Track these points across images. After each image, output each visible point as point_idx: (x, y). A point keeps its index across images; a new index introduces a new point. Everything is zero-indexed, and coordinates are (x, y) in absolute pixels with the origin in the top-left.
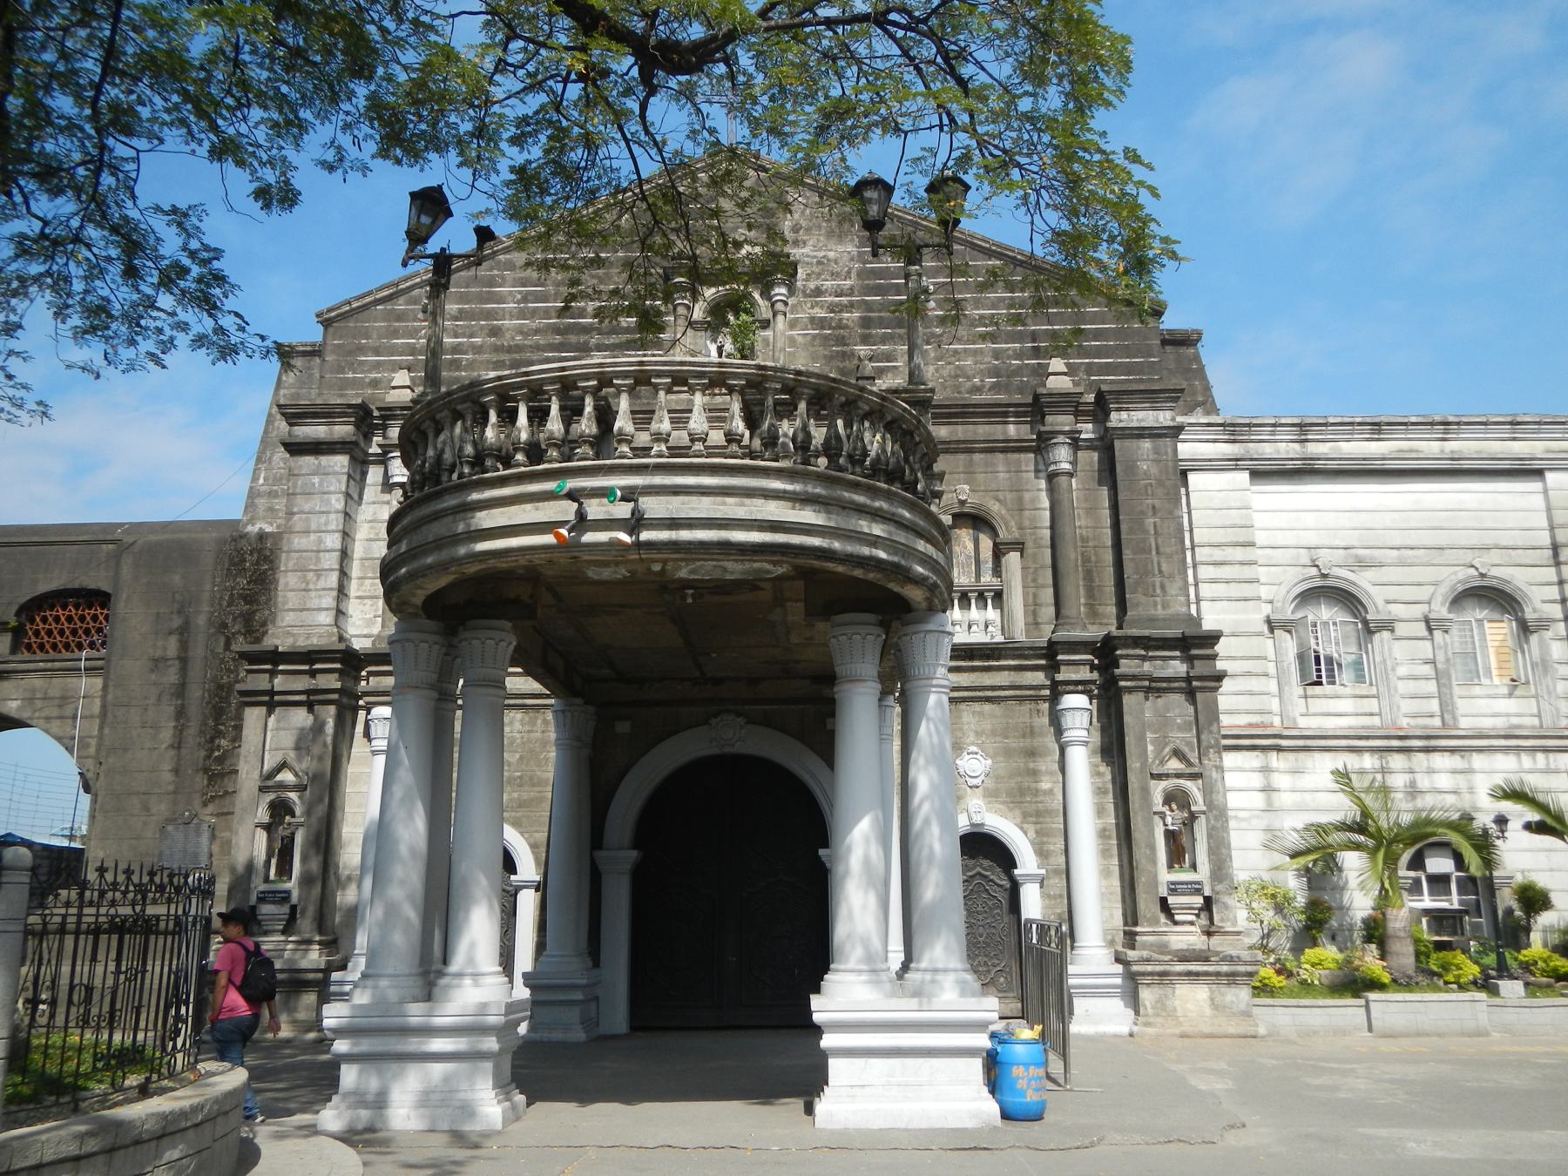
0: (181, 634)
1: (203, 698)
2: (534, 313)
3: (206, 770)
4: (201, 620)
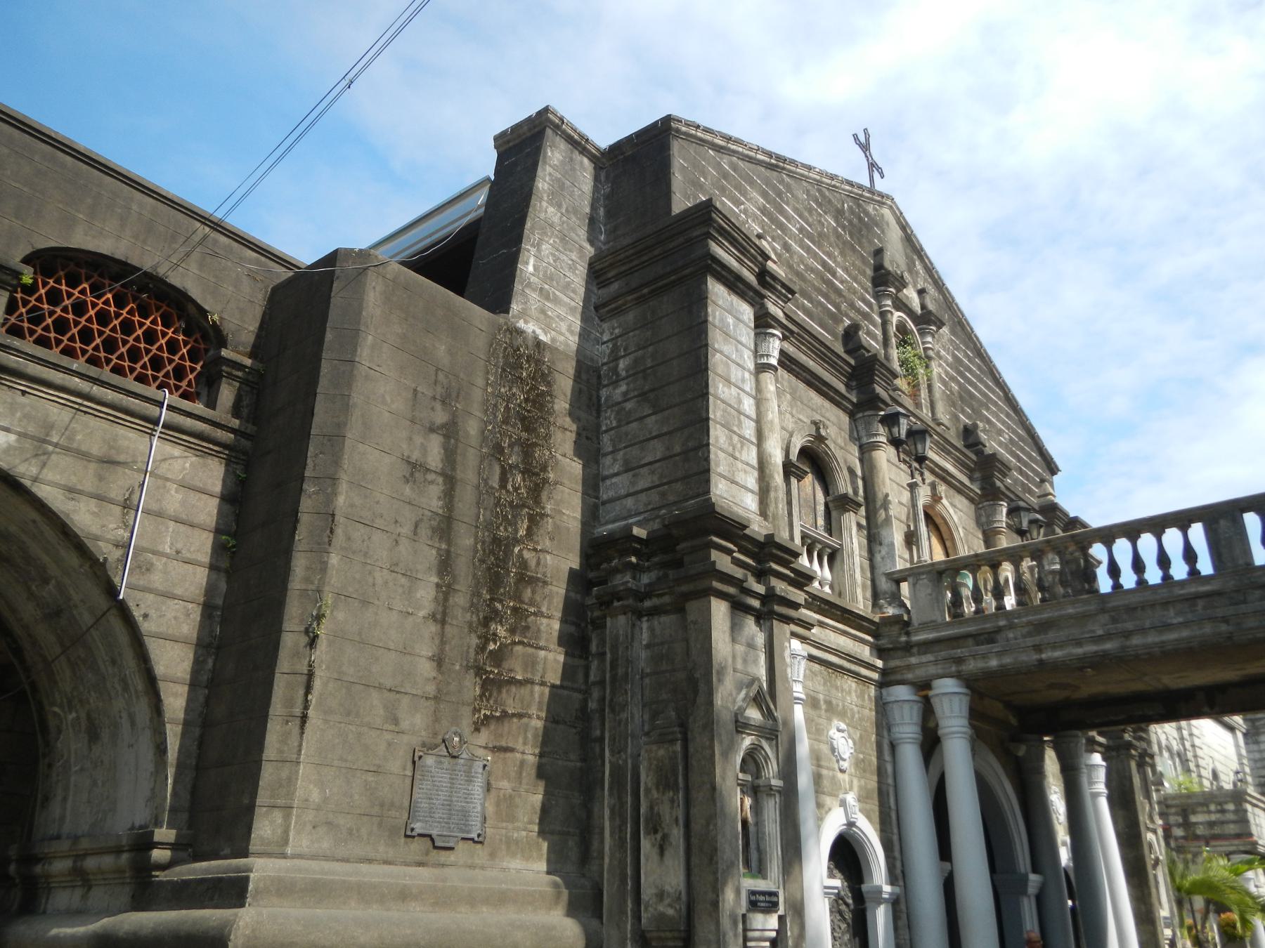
0: (447, 437)
1: (476, 551)
2: (808, 250)
3: (479, 671)
4: (472, 428)
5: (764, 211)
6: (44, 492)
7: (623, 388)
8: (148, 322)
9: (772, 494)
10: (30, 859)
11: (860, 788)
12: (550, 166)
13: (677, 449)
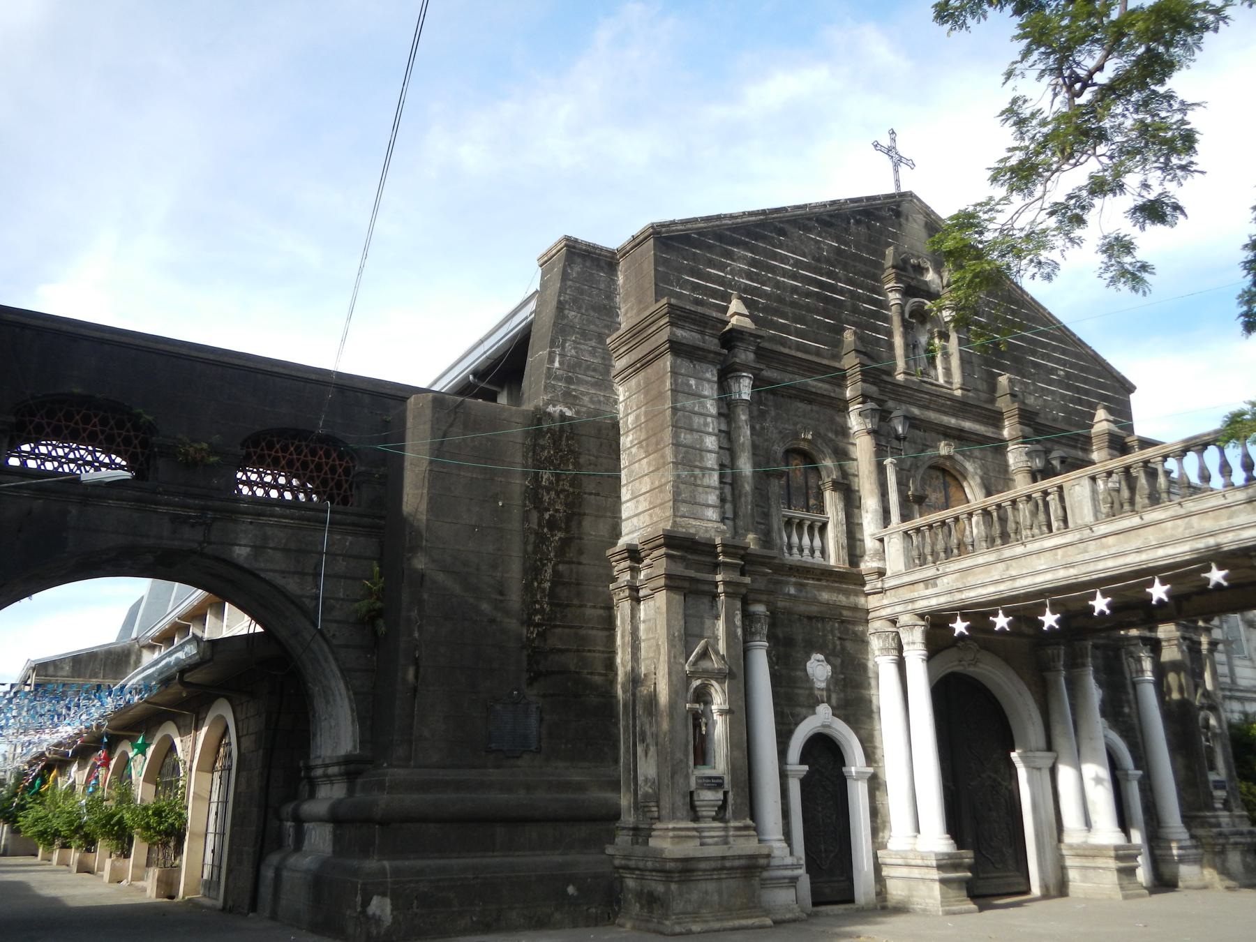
5: (753, 263)
6: (268, 576)
7: (630, 437)
8: (317, 459)
9: (743, 499)
10: (309, 768)
11: (838, 699)
12: (570, 280)
13: (657, 484)
